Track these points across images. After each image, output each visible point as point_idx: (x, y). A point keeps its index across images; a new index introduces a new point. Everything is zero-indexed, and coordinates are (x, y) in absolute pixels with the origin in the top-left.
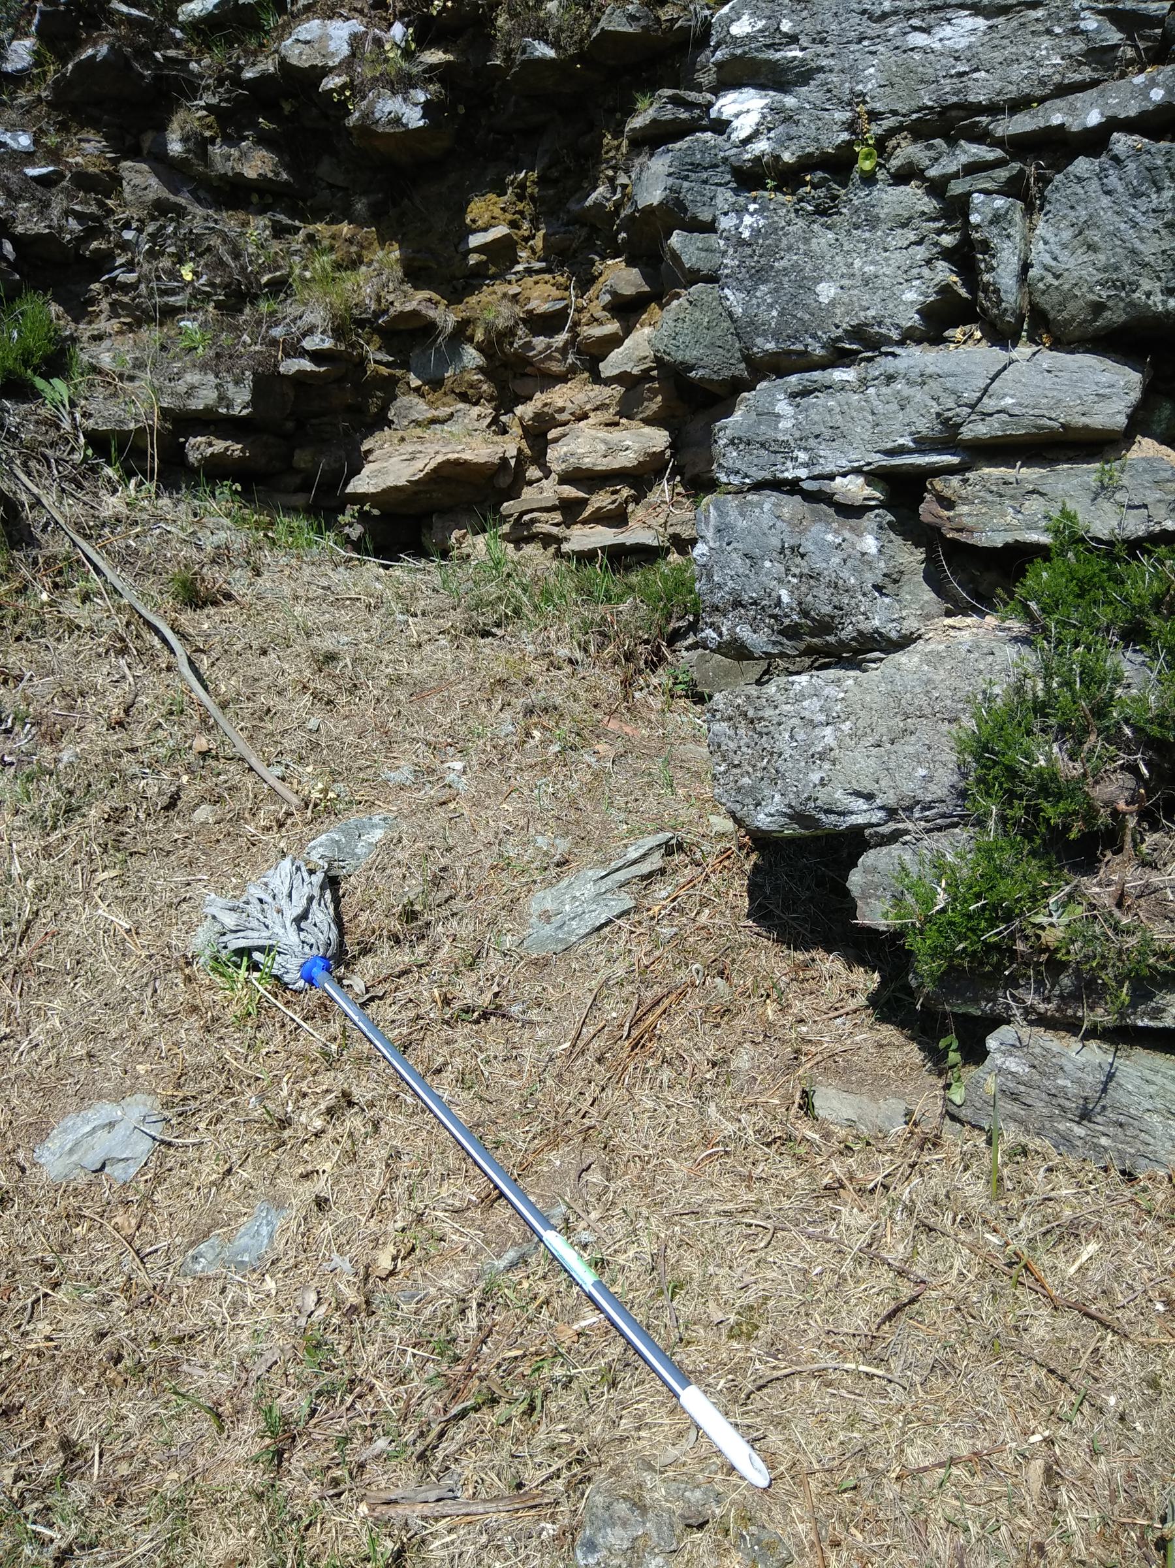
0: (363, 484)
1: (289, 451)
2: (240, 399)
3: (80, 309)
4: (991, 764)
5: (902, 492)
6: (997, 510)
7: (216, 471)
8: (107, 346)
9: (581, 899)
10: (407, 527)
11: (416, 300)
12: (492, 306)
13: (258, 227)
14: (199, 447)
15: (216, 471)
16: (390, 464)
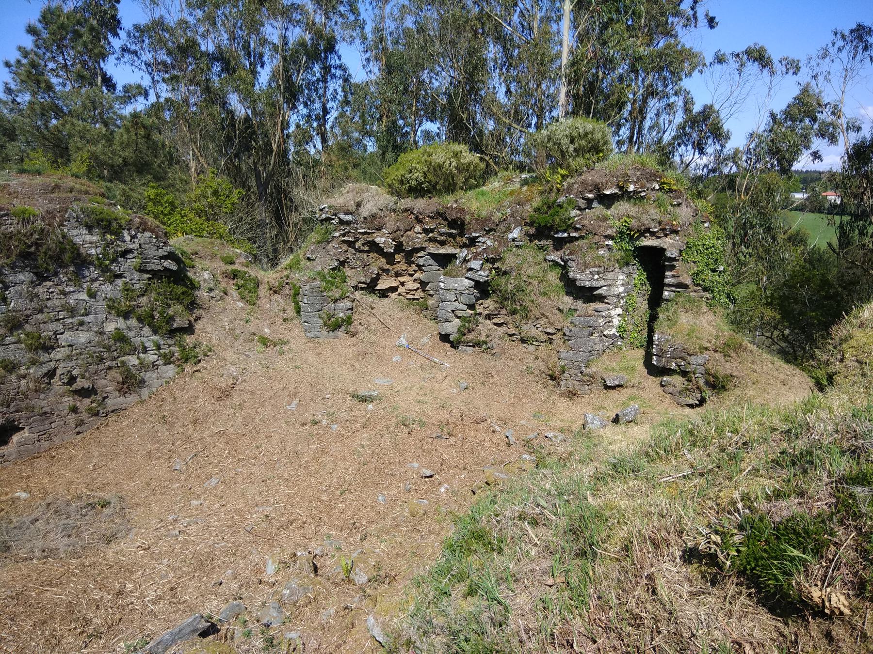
0: (378, 287)
1: (371, 287)
2: (368, 281)
3: (344, 267)
4: (459, 330)
5: (453, 311)
6: (459, 313)
7: (362, 289)
8: (347, 271)
9: (425, 340)
10: (384, 294)
11: (388, 267)
12: (398, 268)
13: (366, 255)
14: (361, 285)
15: (362, 289)
16: (382, 285)
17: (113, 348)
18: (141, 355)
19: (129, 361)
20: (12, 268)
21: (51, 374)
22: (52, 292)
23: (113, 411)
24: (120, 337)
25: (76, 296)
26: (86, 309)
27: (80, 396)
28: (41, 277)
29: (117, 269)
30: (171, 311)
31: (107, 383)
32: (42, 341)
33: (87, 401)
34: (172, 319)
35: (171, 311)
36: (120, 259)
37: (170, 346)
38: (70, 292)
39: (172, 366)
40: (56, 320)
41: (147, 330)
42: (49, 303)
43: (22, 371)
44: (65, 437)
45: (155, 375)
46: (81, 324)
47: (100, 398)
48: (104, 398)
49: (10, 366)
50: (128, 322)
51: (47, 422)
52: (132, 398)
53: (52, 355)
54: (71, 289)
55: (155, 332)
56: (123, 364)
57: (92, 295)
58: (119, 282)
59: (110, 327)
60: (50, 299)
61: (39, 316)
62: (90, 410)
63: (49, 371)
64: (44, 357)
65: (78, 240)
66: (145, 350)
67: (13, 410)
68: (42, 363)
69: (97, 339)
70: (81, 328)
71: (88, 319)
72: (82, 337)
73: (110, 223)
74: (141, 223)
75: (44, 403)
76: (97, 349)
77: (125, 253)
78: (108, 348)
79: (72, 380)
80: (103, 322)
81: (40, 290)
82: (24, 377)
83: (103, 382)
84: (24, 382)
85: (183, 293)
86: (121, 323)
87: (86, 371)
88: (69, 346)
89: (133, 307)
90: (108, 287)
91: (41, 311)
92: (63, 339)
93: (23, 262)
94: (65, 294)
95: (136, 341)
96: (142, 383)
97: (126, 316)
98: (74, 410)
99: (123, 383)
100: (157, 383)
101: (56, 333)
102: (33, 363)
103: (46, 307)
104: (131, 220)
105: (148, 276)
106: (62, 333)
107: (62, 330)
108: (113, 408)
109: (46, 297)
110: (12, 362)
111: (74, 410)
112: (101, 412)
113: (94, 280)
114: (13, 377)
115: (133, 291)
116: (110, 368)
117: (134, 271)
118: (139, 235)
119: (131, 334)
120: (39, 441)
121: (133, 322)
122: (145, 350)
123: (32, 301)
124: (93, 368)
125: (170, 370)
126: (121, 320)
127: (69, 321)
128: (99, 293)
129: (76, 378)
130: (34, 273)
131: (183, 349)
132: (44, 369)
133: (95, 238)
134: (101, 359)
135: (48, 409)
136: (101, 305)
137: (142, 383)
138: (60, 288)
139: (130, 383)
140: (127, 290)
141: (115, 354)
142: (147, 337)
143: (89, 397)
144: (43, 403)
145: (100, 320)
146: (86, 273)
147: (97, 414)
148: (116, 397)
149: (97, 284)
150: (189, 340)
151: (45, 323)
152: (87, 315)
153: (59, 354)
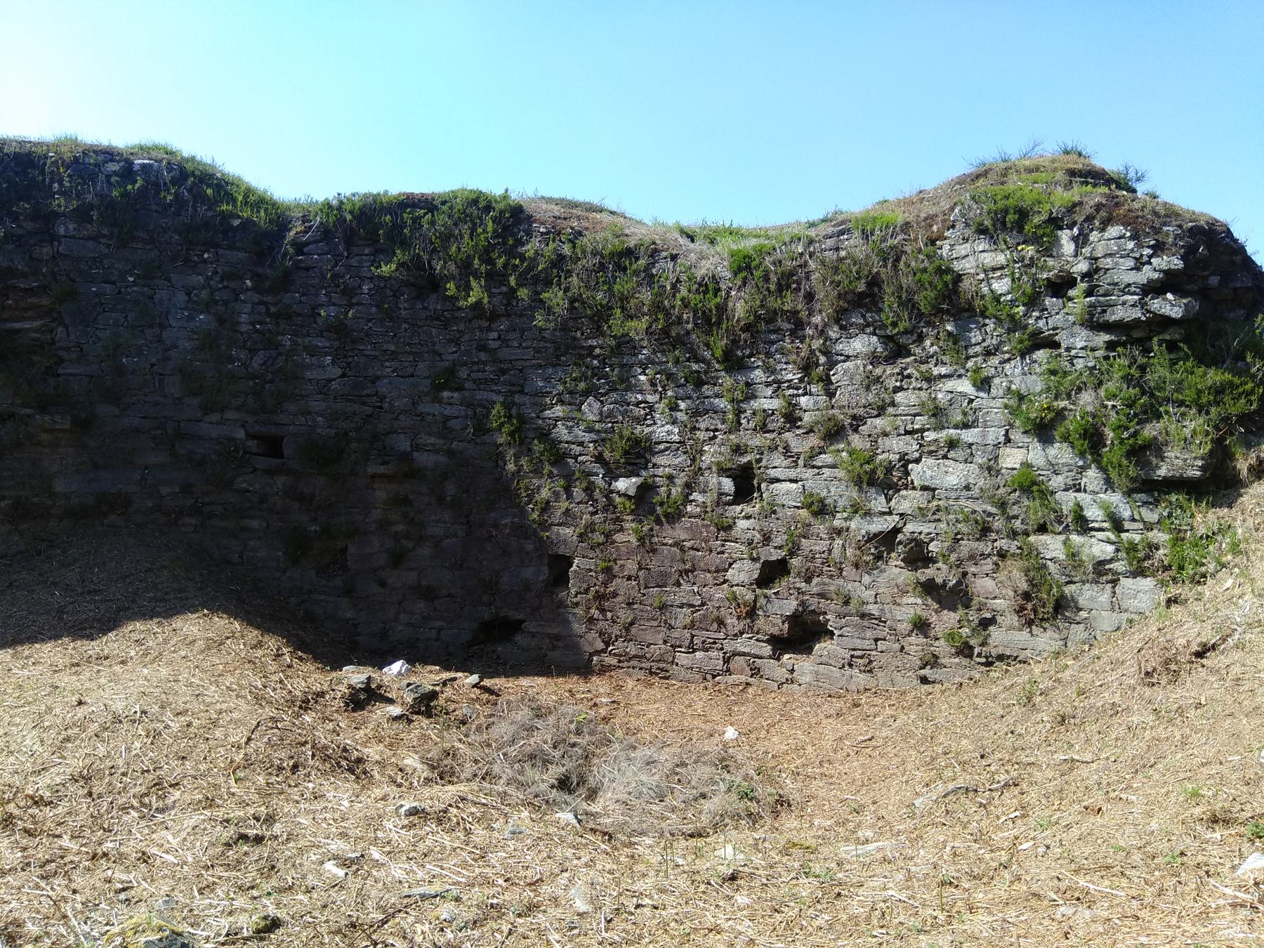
17: (1014, 510)
18: (1075, 538)
19: (1046, 546)
20: (842, 328)
21: (888, 540)
22: (909, 376)
23: (1001, 658)
24: (1030, 485)
25: (950, 385)
26: (965, 414)
27: (939, 602)
28: (896, 351)
29: (1041, 323)
30: (1150, 431)
31: (996, 588)
32: (867, 467)
33: (949, 619)
34: (1155, 448)
35: (1150, 431)
36: (1048, 301)
37: (1149, 527)
38: (941, 377)
39: (1147, 583)
40: (907, 433)
41: (1092, 477)
42: (899, 397)
43: (837, 523)
44: (898, 677)
45: (1104, 597)
46: (952, 444)
47: (974, 617)
48: (986, 623)
49: (814, 508)
50: (1053, 451)
51: (869, 634)
52: (1045, 640)
53: (893, 503)
54: (943, 370)
55: (1109, 484)
56: (1030, 553)
57: (984, 384)
58: (1041, 355)
59: (1012, 459)
60: (901, 389)
61: (878, 421)
62: (951, 637)
63: (881, 533)
64: (879, 503)
65: (967, 266)
66: (1082, 524)
67: (815, 590)
68: (868, 513)
69: (981, 483)
70: (952, 454)
71: (968, 436)
72: (952, 474)
73: (1023, 214)
74: (1099, 207)
75: (868, 595)
76: (980, 507)
77: (1061, 286)
78: (1003, 505)
79: (918, 556)
80: (997, 446)
81: (888, 372)
82: (839, 532)
83: (989, 584)
84: (838, 542)
85: (1219, 390)
86: (1036, 454)
87: (952, 550)
88: (924, 488)
89: (1060, 415)
90: (1014, 368)
91: (881, 411)
92: (921, 472)
93: (863, 316)
94: (930, 379)
95: (1067, 501)
96: (1062, 607)
97: (1043, 430)
98: (921, 626)
99: (1027, 596)
100: (1106, 621)
101: (905, 461)
102: (856, 509)
103: (893, 404)
104: (1081, 203)
105: (1107, 337)
106: (917, 461)
107: (916, 455)
108: (1000, 651)
109: (892, 383)
110: (822, 501)
111: (921, 626)
112: (976, 651)
113: (988, 353)
114: (821, 528)
115: (1065, 373)
116: (1002, 555)
117: (1077, 328)
118: (1094, 236)
119: (1057, 482)
120: (850, 665)
121: (1061, 453)
122: (1082, 524)
123: (868, 388)
124: (967, 546)
125: (1142, 592)
126: (1036, 447)
127: (930, 436)
128: (997, 381)
129: (933, 561)
130: (886, 339)
131: (1178, 540)
132: (880, 525)
133: (1001, 259)
134: (985, 531)
135: (873, 609)
136: (993, 407)
137: (1062, 607)
138: (924, 368)
139: (1047, 606)
140: (1053, 372)
141: (1017, 524)
142: (1098, 496)
143: (953, 608)
144: (861, 588)
145: (991, 439)
146: (975, 337)
147: (965, 651)
148: (1011, 628)
149: (994, 361)
150: (1205, 519)
151: (886, 434)
152: (966, 426)
153: (907, 501)
